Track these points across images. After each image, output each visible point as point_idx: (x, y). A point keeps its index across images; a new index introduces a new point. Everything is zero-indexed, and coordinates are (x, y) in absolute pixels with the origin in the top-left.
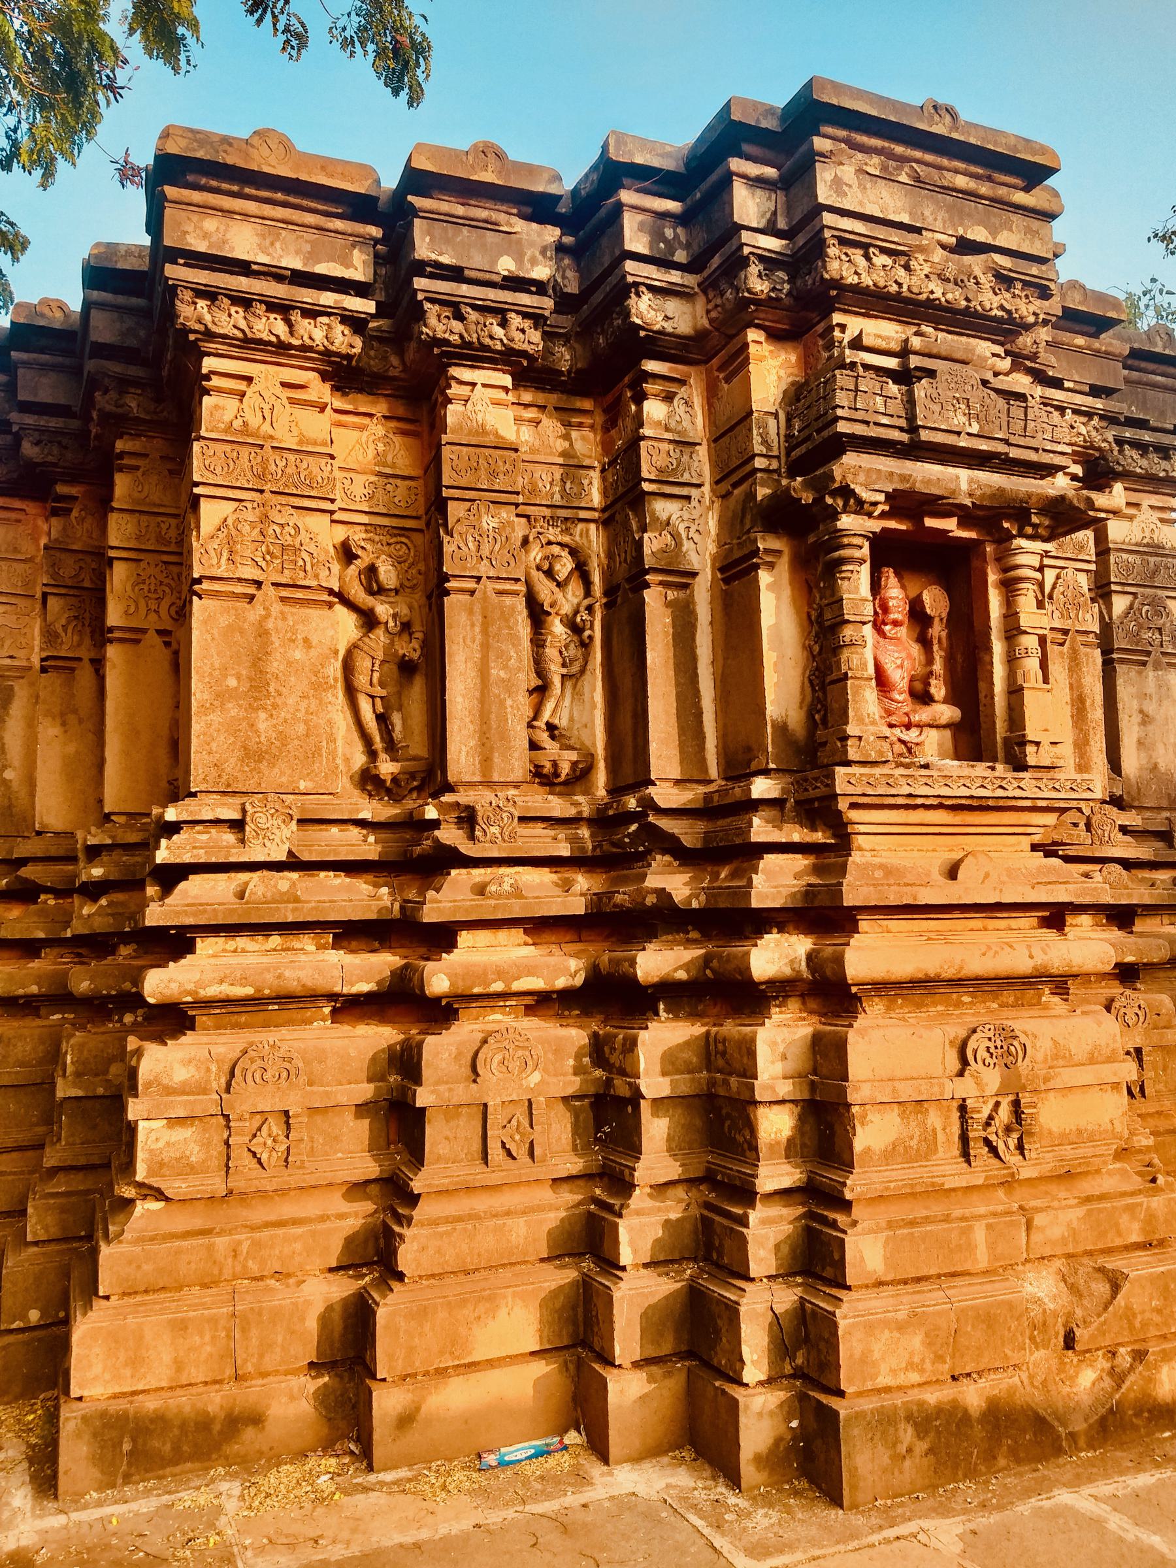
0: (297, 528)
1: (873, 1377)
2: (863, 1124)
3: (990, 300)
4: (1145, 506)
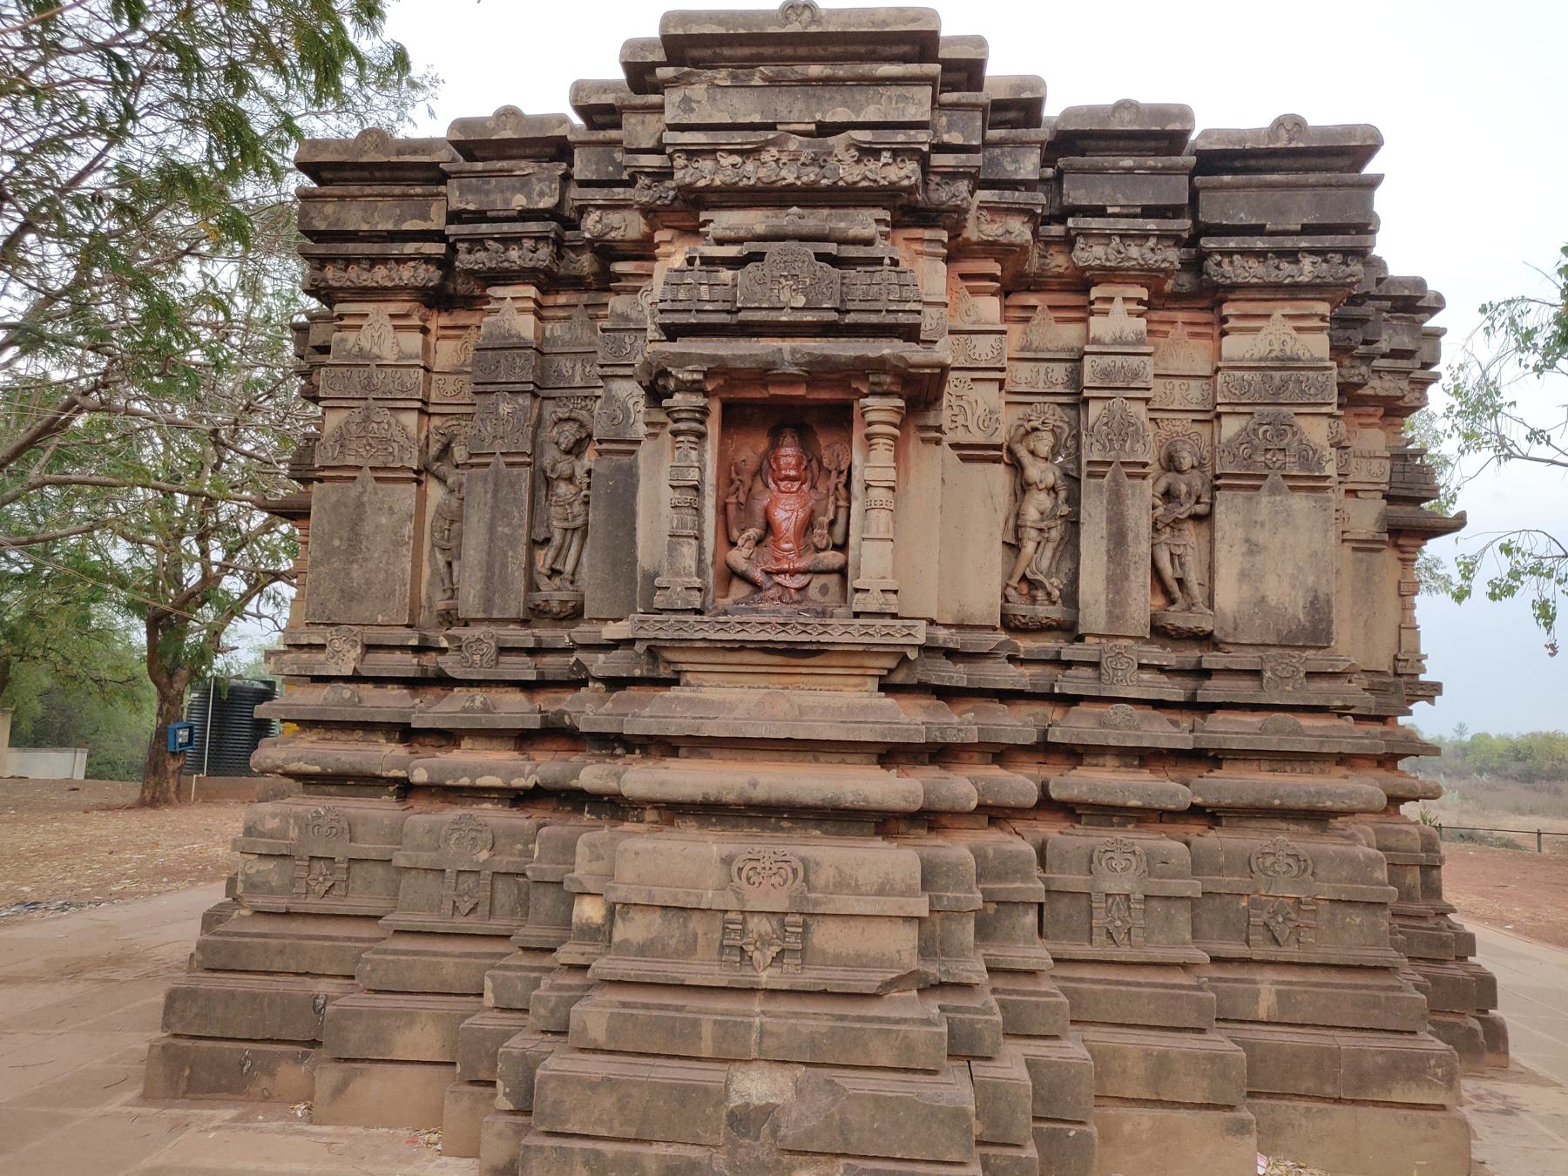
1: (566, 1121)
2: (623, 919)
3: (850, 172)
4: (1277, 314)
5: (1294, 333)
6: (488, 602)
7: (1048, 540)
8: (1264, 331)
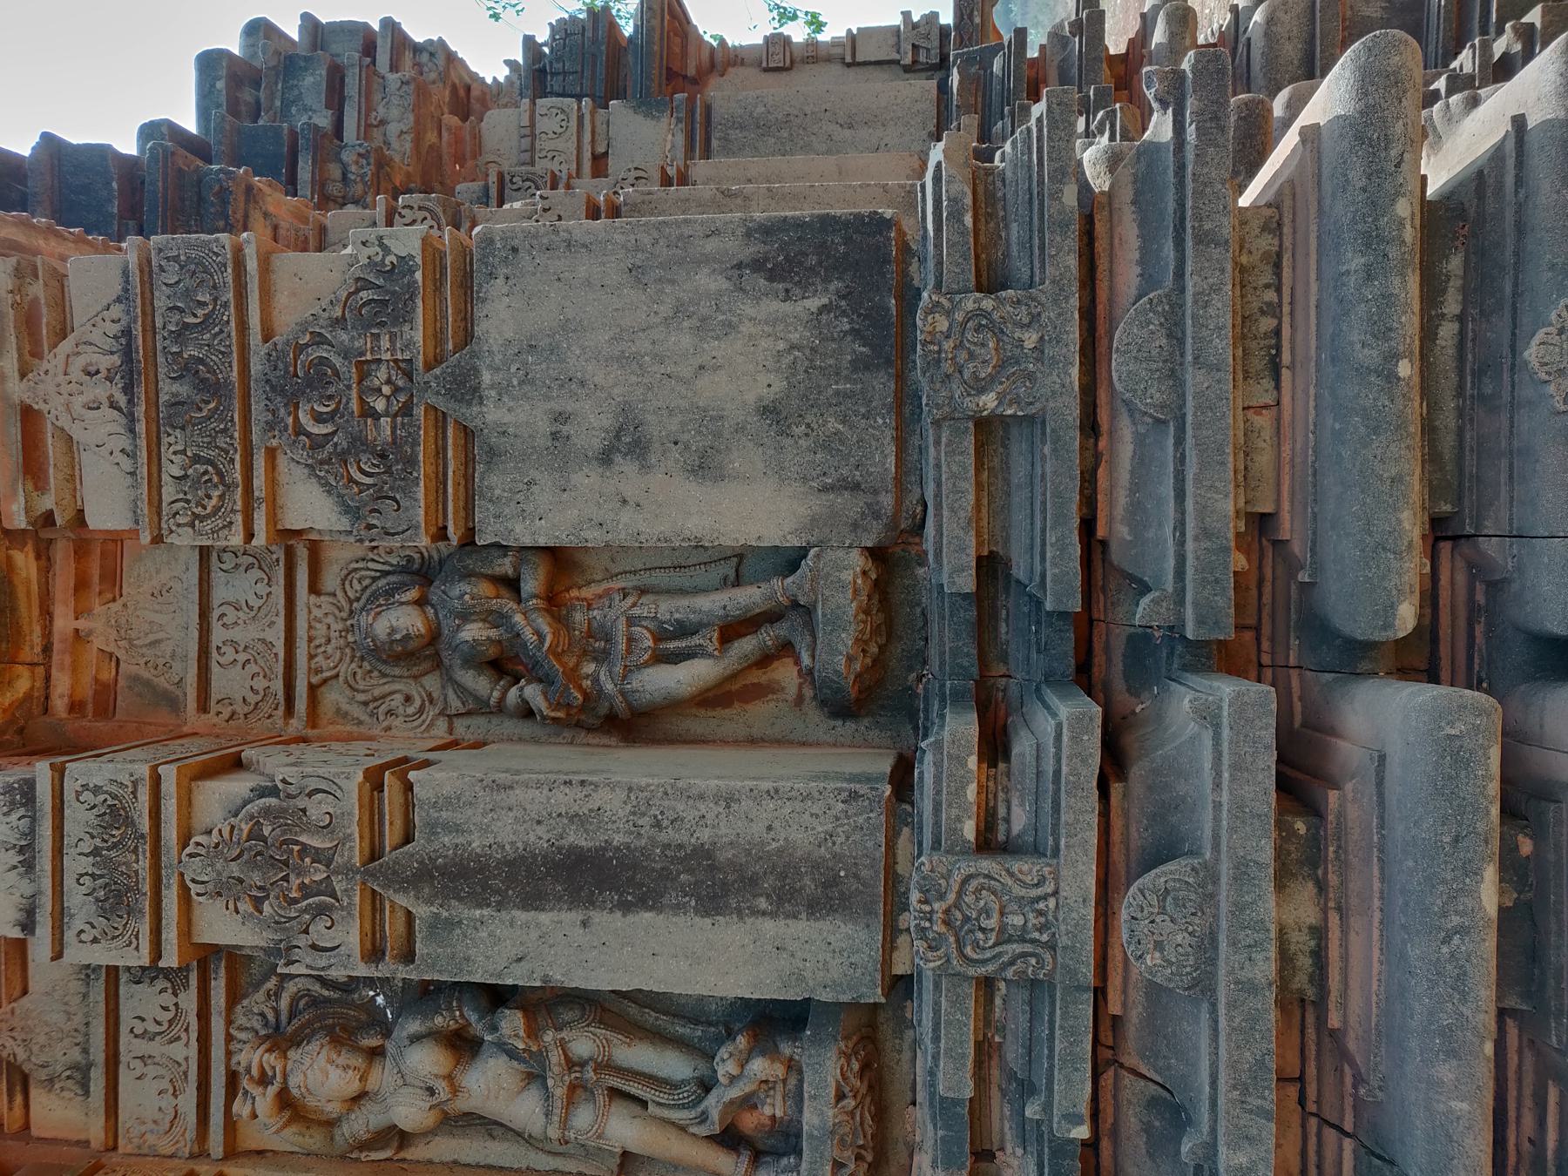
5: (66, 346)
7: (606, 1066)
8: (65, 422)
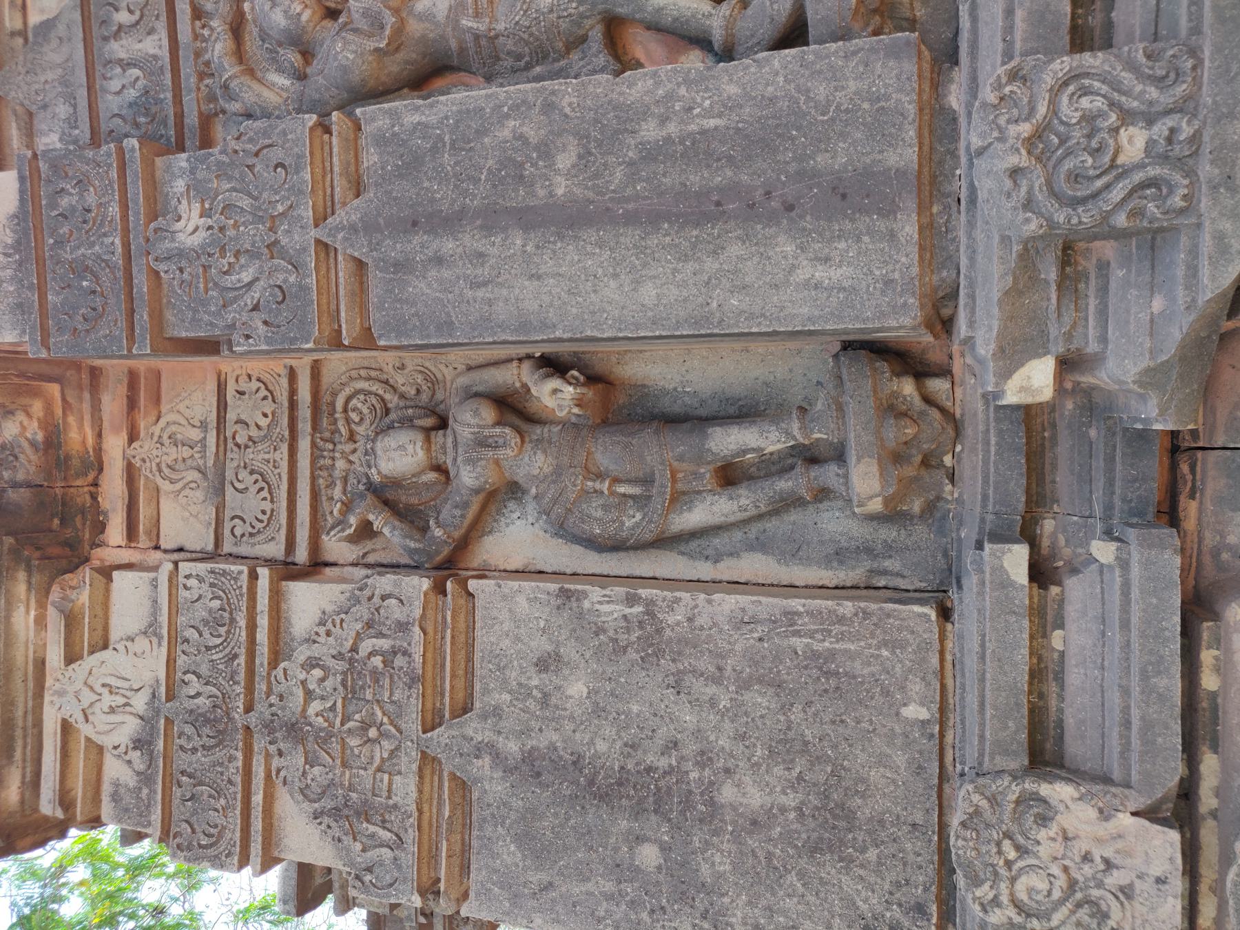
0: (311, 664)
6: (848, 198)
